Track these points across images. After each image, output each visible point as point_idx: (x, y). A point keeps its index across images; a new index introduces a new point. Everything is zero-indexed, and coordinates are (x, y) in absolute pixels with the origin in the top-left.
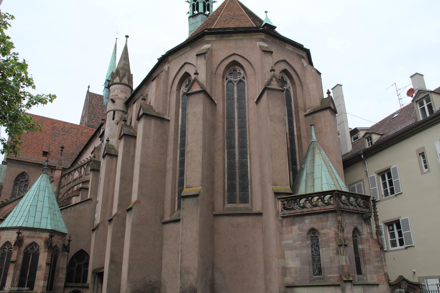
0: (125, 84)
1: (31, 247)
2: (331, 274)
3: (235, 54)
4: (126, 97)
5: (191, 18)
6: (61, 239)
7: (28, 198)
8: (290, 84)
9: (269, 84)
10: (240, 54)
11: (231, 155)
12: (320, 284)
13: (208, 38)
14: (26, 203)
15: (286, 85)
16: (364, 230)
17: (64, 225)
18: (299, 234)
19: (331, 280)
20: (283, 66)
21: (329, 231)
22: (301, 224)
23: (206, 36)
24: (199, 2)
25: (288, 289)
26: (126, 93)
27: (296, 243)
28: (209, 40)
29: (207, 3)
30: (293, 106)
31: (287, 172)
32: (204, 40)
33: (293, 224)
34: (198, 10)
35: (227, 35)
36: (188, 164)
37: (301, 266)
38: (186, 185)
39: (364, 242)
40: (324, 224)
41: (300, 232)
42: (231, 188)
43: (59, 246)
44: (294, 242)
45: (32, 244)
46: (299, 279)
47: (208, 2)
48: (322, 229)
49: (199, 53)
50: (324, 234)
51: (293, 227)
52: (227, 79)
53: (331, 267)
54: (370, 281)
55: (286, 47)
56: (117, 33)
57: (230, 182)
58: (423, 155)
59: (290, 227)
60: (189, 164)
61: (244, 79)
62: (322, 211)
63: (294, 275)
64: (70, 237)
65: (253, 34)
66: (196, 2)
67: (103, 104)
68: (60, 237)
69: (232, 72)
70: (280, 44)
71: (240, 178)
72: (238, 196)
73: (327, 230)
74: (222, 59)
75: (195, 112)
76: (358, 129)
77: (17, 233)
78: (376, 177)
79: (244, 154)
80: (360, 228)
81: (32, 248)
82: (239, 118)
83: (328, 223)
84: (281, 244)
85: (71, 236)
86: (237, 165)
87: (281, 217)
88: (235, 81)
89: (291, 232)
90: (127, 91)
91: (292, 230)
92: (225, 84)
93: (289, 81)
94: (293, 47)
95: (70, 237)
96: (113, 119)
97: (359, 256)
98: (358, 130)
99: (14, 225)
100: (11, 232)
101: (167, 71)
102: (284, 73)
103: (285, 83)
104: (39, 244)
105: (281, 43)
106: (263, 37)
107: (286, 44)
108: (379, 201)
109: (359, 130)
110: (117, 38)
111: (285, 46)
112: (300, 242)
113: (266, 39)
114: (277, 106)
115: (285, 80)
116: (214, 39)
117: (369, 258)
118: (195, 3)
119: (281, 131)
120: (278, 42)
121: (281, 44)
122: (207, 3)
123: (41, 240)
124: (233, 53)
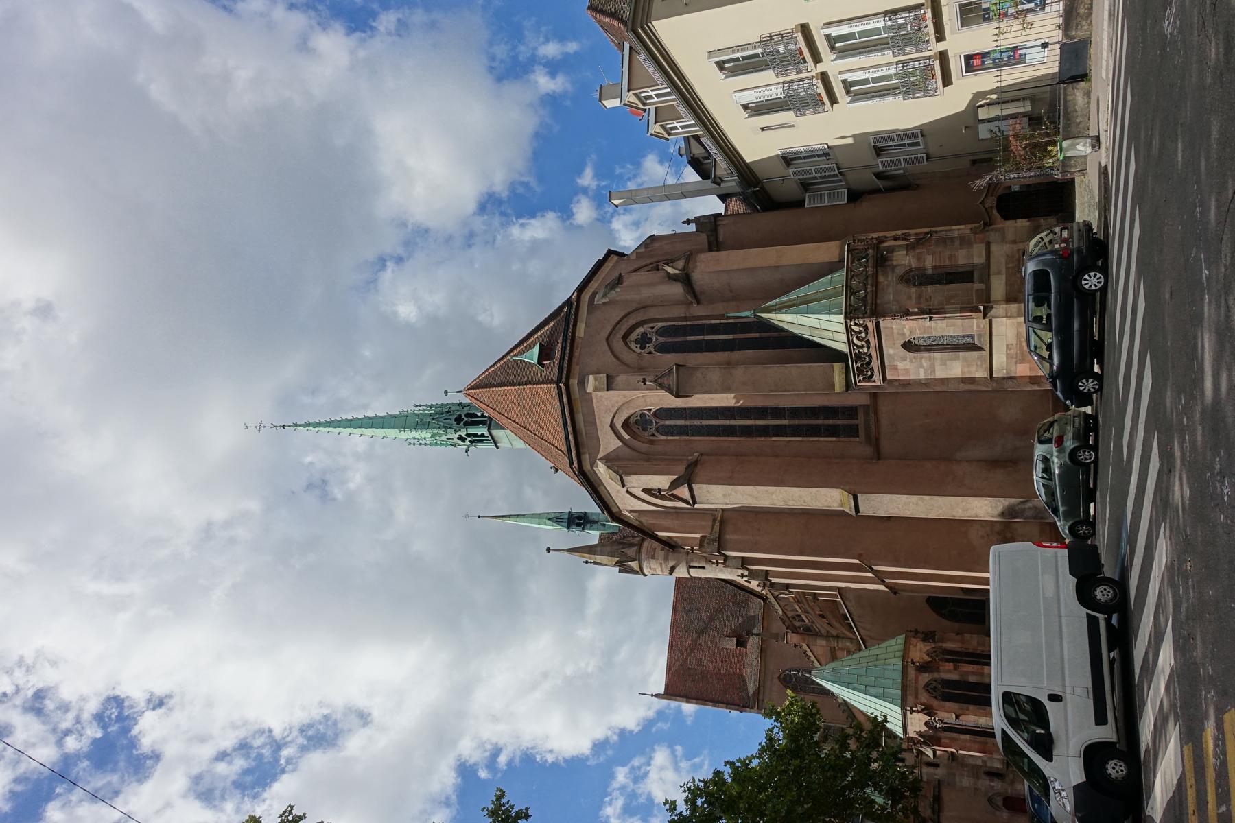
0: (639, 552)
1: (931, 691)
2: (973, 326)
4: (662, 550)
6: (915, 646)
7: (855, 698)
8: (645, 326)
9: (670, 391)
10: (610, 418)
11: (779, 431)
12: (988, 345)
13: (587, 466)
14: (861, 700)
16: (903, 263)
17: (892, 642)
18: (911, 361)
19: (982, 326)
20: (618, 344)
21: (907, 327)
22: (896, 358)
23: (584, 469)
24: (465, 433)
26: (655, 549)
27: (925, 364)
29: (466, 419)
30: (684, 323)
32: (589, 471)
33: (895, 368)
34: (483, 435)
35: (579, 439)
36: (805, 504)
37: (959, 360)
38: (838, 507)
39: (922, 266)
40: (895, 331)
41: (908, 360)
42: (832, 431)
43: (928, 648)
44: (922, 367)
45: (928, 690)
46: (979, 363)
48: (903, 334)
49: (620, 484)
50: (911, 332)
51: (899, 368)
52: (653, 435)
53: (962, 325)
54: (982, 260)
55: (582, 335)
56: (467, 516)
57: (824, 433)
58: (763, 129)
59: (900, 371)
60: (805, 502)
61: (651, 410)
62: (876, 335)
63: (973, 369)
64: (911, 631)
67: (617, 533)
68: (911, 647)
69: (640, 427)
70: (579, 349)
71: (817, 419)
72: (846, 422)
73: (905, 329)
75: (723, 495)
76: (690, 159)
77: (911, 714)
78: (794, 170)
79: (777, 412)
80: (900, 271)
81: (935, 689)
82: (717, 419)
83: (894, 327)
85: (909, 629)
86: (796, 422)
88: (656, 423)
89: (907, 371)
90: (651, 547)
91: (904, 369)
92: (663, 437)
93: (640, 330)
95: (911, 631)
96: (704, 568)
98: (691, 157)
99: (900, 717)
100: (909, 721)
101: (637, 514)
103: (644, 334)
104: (927, 680)
105: (578, 347)
108: (836, 164)
109: (692, 155)
110: (479, 517)
112: (923, 361)
113: (577, 376)
114: (704, 377)
115: (639, 337)
118: (469, 439)
121: (580, 346)
122: (466, 419)
123: (920, 678)
124: (610, 428)
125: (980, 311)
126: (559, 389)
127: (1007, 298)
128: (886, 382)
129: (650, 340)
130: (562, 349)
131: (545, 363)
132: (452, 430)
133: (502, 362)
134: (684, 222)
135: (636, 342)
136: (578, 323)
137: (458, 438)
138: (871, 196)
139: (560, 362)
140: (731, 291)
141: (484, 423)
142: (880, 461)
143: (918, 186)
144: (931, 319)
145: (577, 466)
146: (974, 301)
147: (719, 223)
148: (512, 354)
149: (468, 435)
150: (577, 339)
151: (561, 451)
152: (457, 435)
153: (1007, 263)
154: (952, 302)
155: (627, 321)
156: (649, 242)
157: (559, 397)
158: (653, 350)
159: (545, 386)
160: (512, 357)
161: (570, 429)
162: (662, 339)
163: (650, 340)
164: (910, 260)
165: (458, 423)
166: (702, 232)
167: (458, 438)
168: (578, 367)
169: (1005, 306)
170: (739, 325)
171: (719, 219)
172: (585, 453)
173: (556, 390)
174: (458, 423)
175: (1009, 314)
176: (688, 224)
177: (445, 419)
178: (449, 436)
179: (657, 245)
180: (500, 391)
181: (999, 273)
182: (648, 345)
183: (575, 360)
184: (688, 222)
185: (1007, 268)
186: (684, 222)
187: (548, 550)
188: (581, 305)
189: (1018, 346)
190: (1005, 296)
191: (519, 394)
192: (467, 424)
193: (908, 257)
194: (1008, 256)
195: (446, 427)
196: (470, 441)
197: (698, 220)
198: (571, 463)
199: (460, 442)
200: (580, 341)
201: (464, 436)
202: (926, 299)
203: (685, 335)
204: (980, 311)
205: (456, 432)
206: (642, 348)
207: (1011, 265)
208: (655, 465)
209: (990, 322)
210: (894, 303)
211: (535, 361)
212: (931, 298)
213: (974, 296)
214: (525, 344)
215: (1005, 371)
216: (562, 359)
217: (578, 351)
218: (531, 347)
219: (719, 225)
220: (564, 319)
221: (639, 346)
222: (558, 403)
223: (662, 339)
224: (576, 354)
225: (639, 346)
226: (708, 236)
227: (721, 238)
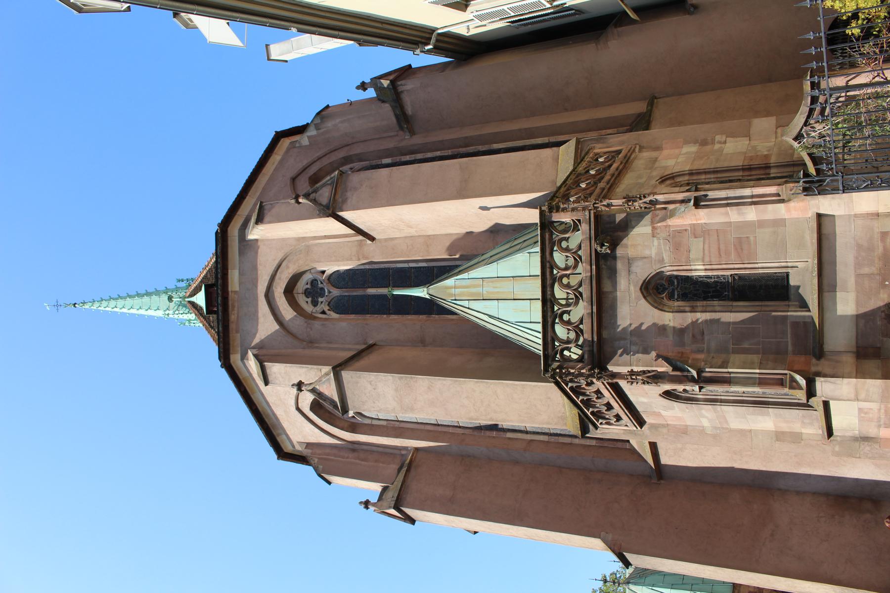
3: (298, 409)
15: (319, 283)
16: (647, 253)
25: (835, 433)
31: (524, 385)
65: (241, 378)
74: (317, 430)
84: (714, 436)
87: (641, 428)
94: (229, 271)
97: (728, 276)
102: (294, 292)
105: (233, 307)
111: (236, 292)
113: (239, 349)
114: (375, 389)
115: (309, 286)
117: (734, 245)
119: (429, 388)
121: (236, 304)
124: (297, 412)
125: (800, 388)
127: (857, 347)
128: (645, 427)
129: (321, 293)
134: (358, 88)
135: (307, 293)
138: (620, 29)
140: (411, 227)
142: (662, 482)
143: (695, 7)
144: (701, 388)
146: (790, 348)
147: (400, 89)
150: (231, 296)
153: (858, 265)
154: (746, 345)
155: (288, 267)
156: (318, 121)
158: (326, 308)
162: (336, 292)
163: (321, 293)
164: (659, 245)
166: (383, 102)
168: (239, 335)
169: (854, 380)
170: (435, 269)
171: (399, 83)
172: (279, 435)
175: (862, 395)
176: (365, 89)
179: (329, 124)
181: (845, 290)
182: (320, 300)
184: (363, 86)
185: (858, 276)
186: (358, 88)
189: (883, 411)
190: (854, 342)
193: (656, 242)
194: (859, 247)
197: (375, 82)
200: (236, 296)
202: (694, 336)
203: (365, 286)
204: (800, 388)
206: (315, 303)
207: (866, 270)
208: (362, 460)
209: (826, 405)
210: (634, 339)
212: (703, 334)
213: (789, 336)
215: (857, 432)
217: (236, 312)
219: (402, 92)
221: (309, 300)
223: (336, 292)
225: (309, 300)
226: (392, 107)
227: (409, 111)
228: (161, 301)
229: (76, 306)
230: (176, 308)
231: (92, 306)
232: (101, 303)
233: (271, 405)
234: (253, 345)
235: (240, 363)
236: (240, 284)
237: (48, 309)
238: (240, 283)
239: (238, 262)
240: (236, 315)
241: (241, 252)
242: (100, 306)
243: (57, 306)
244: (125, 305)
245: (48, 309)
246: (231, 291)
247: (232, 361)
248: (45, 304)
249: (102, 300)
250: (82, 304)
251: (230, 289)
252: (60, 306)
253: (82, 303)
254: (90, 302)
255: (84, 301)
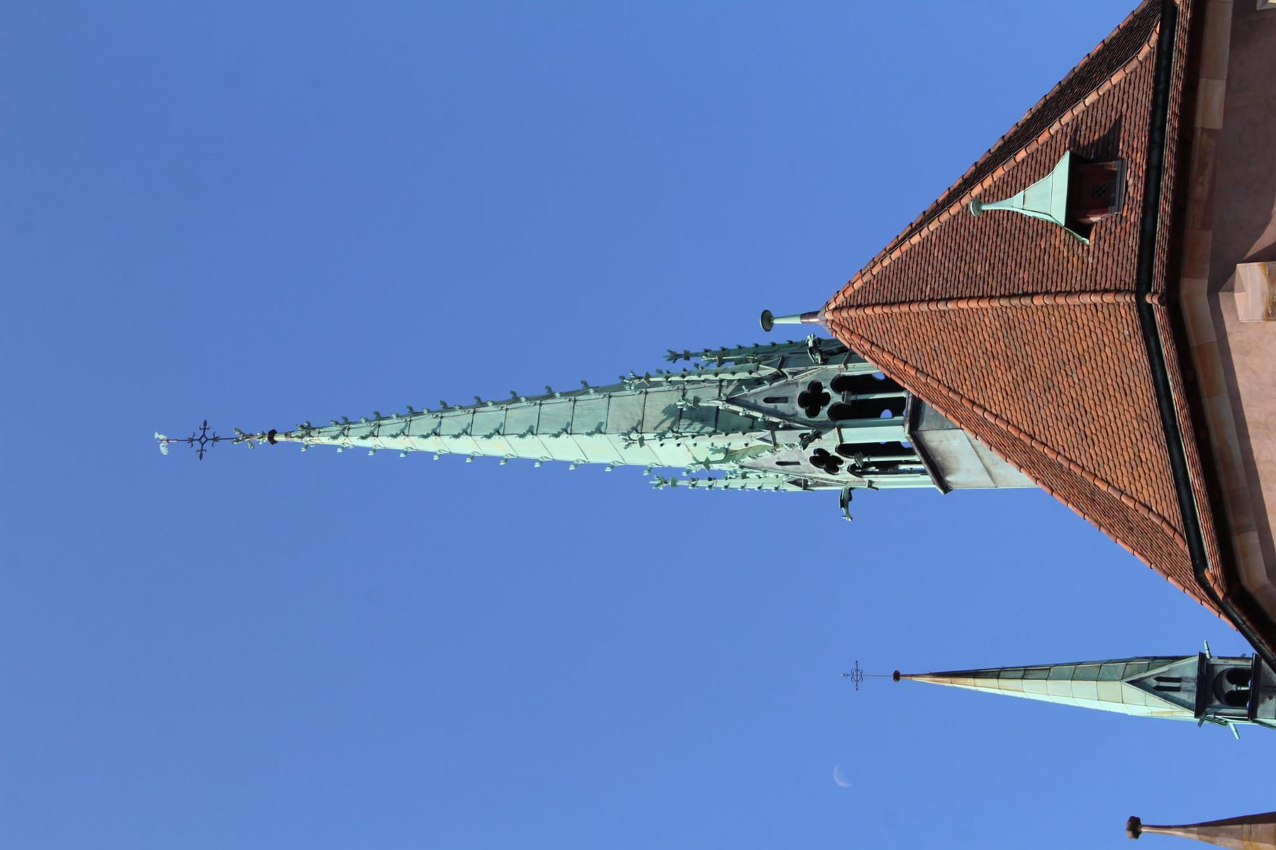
5: (948, 478)
28: (1263, 566)
29: (836, 398)
34: (894, 448)
47: (825, 391)
56: (857, 675)
66: (843, 458)
70: (1208, 171)
106: (1202, 285)
107: (1199, 132)
111: (1212, 133)
113: (1208, 266)
116: (1253, 538)
118: (849, 462)
120: (1202, 184)
122: (836, 398)
126: (1145, 313)
130: (1148, 172)
131: (1094, 219)
132: (794, 436)
133: (945, 217)
136: (1203, 81)
137: (815, 461)
139: (1143, 221)
141: (896, 407)
145: (1218, 572)
148: (977, 190)
149: (846, 449)
150: (1200, 139)
151: (1164, 519)
152: (810, 451)
157: (1145, 337)
159: (1096, 299)
160: (979, 201)
161: (1188, 449)
165: (813, 412)
167: (815, 461)
172: (1244, 529)
173: (1135, 314)
174: (813, 412)
177: (766, 400)
178: (783, 454)
180: (943, 314)
183: (1195, 212)
187: (1135, 826)
188: (1209, 15)
191: (1010, 326)
192: (842, 415)
195: (773, 427)
196: (852, 469)
198: (1199, 562)
199: (821, 474)
201: (833, 452)
205: (806, 441)
211: (1058, 215)
214: (1021, 155)
216: (1150, 207)
218: (1042, 168)
220: (1151, 66)
222: (1144, 361)
224: (1200, 190)
228: (612, 407)
229: (276, 438)
230: (667, 424)
231: (342, 433)
232: (379, 426)
233: (1251, 431)
234: (1250, 253)
235: (1203, 303)
236: (1226, 114)
237: (164, 451)
238: (1228, 111)
239: (1226, 62)
240: (1207, 187)
241: (1237, 39)
242: (372, 434)
243: (204, 439)
244: (470, 425)
245: (164, 451)
246: (1203, 129)
247: (1184, 292)
248: (157, 435)
249: (379, 418)
250: (304, 432)
251: (1199, 123)
252: (215, 439)
253: (302, 427)
254: (337, 423)
255: (309, 424)
